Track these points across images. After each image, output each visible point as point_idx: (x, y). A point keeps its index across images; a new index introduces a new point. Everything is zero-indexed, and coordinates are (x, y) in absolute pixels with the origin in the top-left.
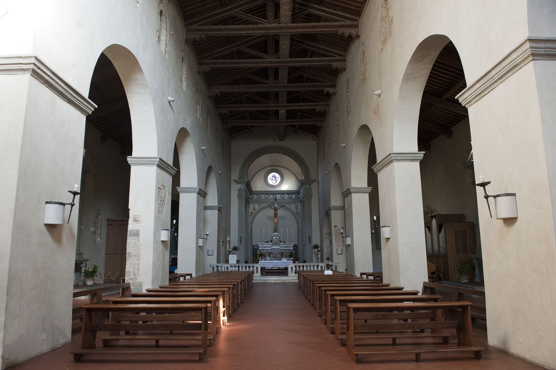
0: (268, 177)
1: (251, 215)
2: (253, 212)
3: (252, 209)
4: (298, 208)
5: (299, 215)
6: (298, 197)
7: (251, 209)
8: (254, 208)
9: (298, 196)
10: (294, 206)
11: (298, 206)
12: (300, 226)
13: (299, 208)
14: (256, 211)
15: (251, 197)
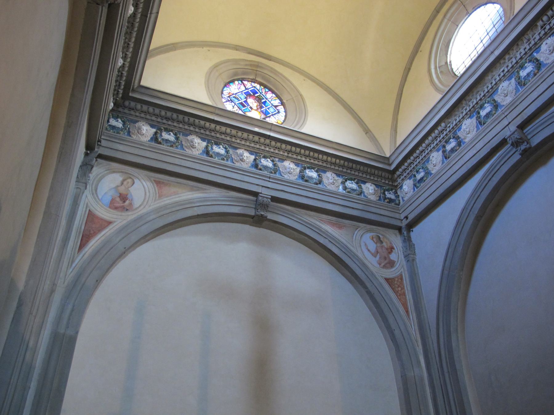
0: (226, 91)
1: (85, 239)
2: (103, 213)
3: (108, 199)
4: (393, 257)
5: (401, 296)
6: (391, 201)
7: (95, 192)
8: (124, 198)
10: (372, 246)
11: (391, 249)
12: (419, 362)
13: (397, 256)
14: (130, 216)
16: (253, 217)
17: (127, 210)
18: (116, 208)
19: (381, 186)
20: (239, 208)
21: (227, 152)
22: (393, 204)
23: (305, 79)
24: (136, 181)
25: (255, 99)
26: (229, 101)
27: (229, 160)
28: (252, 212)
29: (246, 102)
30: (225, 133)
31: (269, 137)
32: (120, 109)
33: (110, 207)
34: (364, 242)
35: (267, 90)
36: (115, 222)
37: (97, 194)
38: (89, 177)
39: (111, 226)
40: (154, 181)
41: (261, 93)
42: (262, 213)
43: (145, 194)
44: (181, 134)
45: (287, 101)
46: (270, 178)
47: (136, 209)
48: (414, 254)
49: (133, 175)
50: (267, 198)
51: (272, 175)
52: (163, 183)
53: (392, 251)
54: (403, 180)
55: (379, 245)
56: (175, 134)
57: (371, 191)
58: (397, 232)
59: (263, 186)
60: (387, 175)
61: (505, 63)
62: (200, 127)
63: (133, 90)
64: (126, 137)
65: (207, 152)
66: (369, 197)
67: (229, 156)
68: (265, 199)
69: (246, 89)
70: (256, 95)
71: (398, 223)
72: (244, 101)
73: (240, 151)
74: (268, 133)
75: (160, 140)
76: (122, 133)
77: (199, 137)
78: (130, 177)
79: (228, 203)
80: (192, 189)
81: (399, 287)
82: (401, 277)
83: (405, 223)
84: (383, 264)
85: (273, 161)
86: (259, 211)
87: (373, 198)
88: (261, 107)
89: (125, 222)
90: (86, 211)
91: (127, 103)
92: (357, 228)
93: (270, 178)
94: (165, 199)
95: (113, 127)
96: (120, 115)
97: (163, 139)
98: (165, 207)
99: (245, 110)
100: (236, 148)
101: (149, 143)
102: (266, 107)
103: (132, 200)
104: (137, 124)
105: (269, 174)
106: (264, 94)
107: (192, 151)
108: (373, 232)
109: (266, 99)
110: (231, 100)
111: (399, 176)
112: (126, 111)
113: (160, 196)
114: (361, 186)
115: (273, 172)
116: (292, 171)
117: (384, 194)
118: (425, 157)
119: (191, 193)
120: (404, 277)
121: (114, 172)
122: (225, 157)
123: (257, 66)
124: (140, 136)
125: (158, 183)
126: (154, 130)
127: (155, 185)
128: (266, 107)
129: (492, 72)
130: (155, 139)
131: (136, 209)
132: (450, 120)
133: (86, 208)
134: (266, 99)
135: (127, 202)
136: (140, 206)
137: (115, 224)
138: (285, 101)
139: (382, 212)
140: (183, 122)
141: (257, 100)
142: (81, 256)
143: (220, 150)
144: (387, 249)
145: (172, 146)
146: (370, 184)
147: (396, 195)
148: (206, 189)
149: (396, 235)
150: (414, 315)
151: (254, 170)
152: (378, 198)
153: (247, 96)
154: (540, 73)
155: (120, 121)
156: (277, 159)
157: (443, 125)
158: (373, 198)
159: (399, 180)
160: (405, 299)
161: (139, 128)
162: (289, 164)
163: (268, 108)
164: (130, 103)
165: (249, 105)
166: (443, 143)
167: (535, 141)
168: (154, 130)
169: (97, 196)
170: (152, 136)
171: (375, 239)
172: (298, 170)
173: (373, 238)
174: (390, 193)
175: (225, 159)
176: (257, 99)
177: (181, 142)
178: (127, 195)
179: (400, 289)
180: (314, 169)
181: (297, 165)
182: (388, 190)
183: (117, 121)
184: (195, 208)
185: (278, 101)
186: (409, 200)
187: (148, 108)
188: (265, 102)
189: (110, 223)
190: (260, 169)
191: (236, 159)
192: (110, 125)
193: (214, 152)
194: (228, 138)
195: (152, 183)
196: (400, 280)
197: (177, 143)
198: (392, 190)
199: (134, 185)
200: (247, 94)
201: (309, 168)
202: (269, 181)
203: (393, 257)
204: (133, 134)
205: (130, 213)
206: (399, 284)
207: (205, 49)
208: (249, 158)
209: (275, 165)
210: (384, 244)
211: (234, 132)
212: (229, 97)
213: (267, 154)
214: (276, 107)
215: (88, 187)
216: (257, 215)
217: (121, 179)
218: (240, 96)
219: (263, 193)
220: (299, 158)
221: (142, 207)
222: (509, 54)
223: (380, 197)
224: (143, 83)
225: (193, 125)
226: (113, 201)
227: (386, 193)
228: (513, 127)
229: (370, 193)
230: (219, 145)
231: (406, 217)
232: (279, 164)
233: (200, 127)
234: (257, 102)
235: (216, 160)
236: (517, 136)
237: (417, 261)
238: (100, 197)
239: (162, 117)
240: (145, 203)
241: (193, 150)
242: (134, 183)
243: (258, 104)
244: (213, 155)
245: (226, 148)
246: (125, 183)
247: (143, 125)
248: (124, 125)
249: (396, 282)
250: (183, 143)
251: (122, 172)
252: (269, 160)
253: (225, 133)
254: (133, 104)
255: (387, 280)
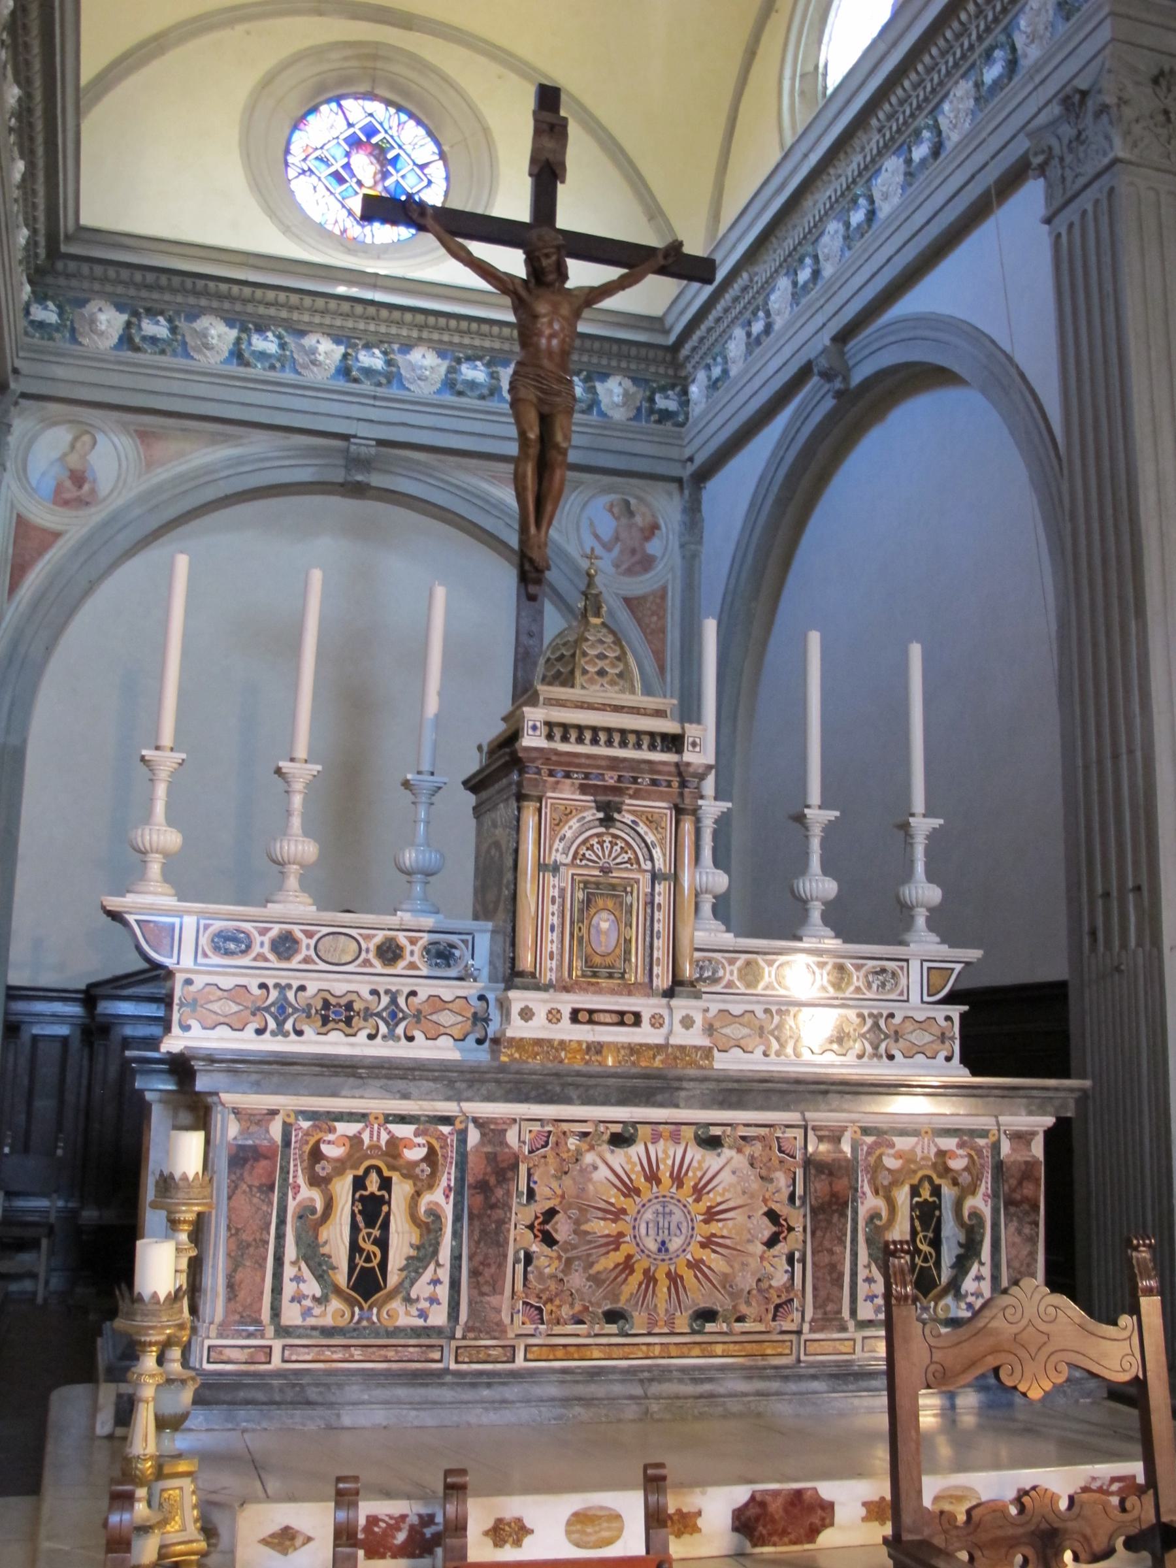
0: (299, 141)
2: (44, 516)
3: (49, 485)
4: (654, 547)
6: (665, 416)
8: (78, 478)
9: (661, 402)
10: (607, 526)
14: (95, 516)
15: (48, 314)
16: (342, 485)
17: (87, 504)
18: (66, 503)
19: (647, 381)
20: (311, 470)
21: (283, 346)
22: (668, 426)
23: (505, 72)
24: (100, 437)
25: (371, 154)
26: (304, 172)
27: (287, 367)
28: (339, 476)
29: (347, 166)
30: (275, 304)
31: (372, 303)
32: (49, 280)
33: (55, 503)
34: (590, 520)
35: (404, 117)
36: (66, 532)
37: (27, 479)
38: (8, 444)
39: (60, 542)
40: (136, 431)
41: (386, 132)
42: (359, 478)
43: (120, 465)
44: (183, 315)
45: (452, 147)
46: (375, 398)
47: (104, 499)
48: (700, 542)
49: (91, 425)
50: (368, 446)
51: (380, 391)
52: (153, 433)
53: (653, 534)
54: (694, 367)
55: (624, 521)
56: (170, 320)
57: (616, 399)
58: (674, 487)
59: (359, 420)
60: (660, 354)
61: (830, 182)
62: (220, 297)
63: (68, 238)
64: (68, 345)
65: (238, 355)
66: (610, 413)
67: (285, 356)
68: (363, 450)
69: (350, 125)
70: (374, 140)
71: (675, 471)
72: (343, 167)
73: (309, 341)
74: (369, 295)
75: (137, 340)
76: (57, 335)
77: (222, 318)
78: (85, 430)
79: (287, 463)
80: (215, 440)
81: (653, 614)
82: (662, 594)
83: (691, 468)
84: (624, 567)
85: (385, 353)
86: (353, 472)
87: (619, 415)
88: (385, 175)
89: (85, 530)
90: (11, 517)
91: (60, 265)
92: (576, 488)
93: (375, 398)
94: (159, 470)
95: (41, 325)
96: (50, 293)
97: (144, 338)
98: (159, 488)
99: (345, 194)
100: (302, 333)
101: (116, 353)
102: (398, 171)
103: (95, 481)
104: (88, 306)
105: (373, 388)
106: (395, 134)
107: (206, 356)
108: (615, 492)
109: (400, 147)
110: (310, 169)
111: (688, 358)
112: (62, 281)
113: (150, 465)
114: (594, 387)
115: (384, 381)
116: (427, 373)
117: (651, 400)
118: (724, 331)
119: (210, 450)
120: (670, 594)
121: (55, 424)
122: (279, 360)
123: (375, 57)
124: (96, 337)
125: (144, 436)
126: (125, 317)
127: (138, 441)
128: (398, 171)
129: (812, 193)
130: (127, 340)
131: (104, 499)
132: (756, 269)
133: (11, 511)
134: (400, 147)
135: (86, 487)
136: (112, 491)
137: (68, 536)
138: (446, 148)
139: (639, 448)
140: (183, 290)
141: (375, 157)
142: (14, 605)
143: (266, 344)
144: (642, 530)
145: (163, 352)
146: (618, 378)
147: (684, 398)
148: (241, 437)
149: (670, 494)
150: (677, 673)
151: (342, 384)
152: (632, 414)
153: (350, 146)
154: (870, 233)
155: (50, 304)
156: (396, 347)
157: (745, 275)
158: (619, 415)
159: (689, 367)
160: (663, 641)
161: (93, 321)
162: (424, 356)
163: (403, 177)
164: (66, 265)
165: (354, 175)
166: (748, 315)
167: (857, 378)
168: (125, 317)
169: (29, 483)
170: (121, 332)
171: (616, 510)
172: (443, 366)
173: (612, 505)
174: (667, 397)
175: (278, 365)
176: (376, 152)
177: (183, 336)
178: (84, 472)
179: (655, 619)
180: (480, 358)
181: (441, 354)
182: (663, 389)
183: (46, 308)
184: (221, 483)
185: (432, 147)
186: (705, 413)
187: (106, 271)
188: (397, 157)
189: (57, 535)
190: (356, 380)
191: (301, 361)
192: (32, 322)
193: (254, 352)
194: (284, 314)
195: (132, 437)
196: (658, 601)
197: (177, 344)
198: (673, 387)
199: (97, 447)
200: (351, 141)
201: (469, 359)
202: (374, 406)
203: (654, 547)
204: (81, 334)
205: (93, 510)
206: (654, 608)
207: (240, 28)
208: (328, 351)
209: (389, 363)
210: (638, 519)
211: (294, 299)
212: (305, 160)
213: (372, 339)
214: (422, 167)
215: (8, 465)
216: (349, 483)
217: (69, 437)
218: (333, 151)
219: (360, 434)
220: (446, 338)
221: (115, 494)
222: (835, 167)
223: (639, 409)
224: (84, 221)
225: (206, 293)
226: (59, 489)
227: (658, 397)
228: (825, 339)
229: (613, 403)
230: (265, 331)
231: (691, 459)
232: (399, 358)
233: (220, 297)
234: (374, 161)
235: (258, 370)
236: (824, 363)
237: (703, 557)
238: (34, 483)
239: (138, 286)
240: (120, 484)
241: (208, 353)
242: (95, 443)
243: (379, 168)
244: (252, 360)
245: (279, 337)
246: (78, 445)
247: (100, 310)
248: (60, 315)
249: (648, 605)
250: (188, 339)
251: (70, 422)
252: (377, 351)
253: (275, 304)
254: (72, 266)
255: (628, 601)
